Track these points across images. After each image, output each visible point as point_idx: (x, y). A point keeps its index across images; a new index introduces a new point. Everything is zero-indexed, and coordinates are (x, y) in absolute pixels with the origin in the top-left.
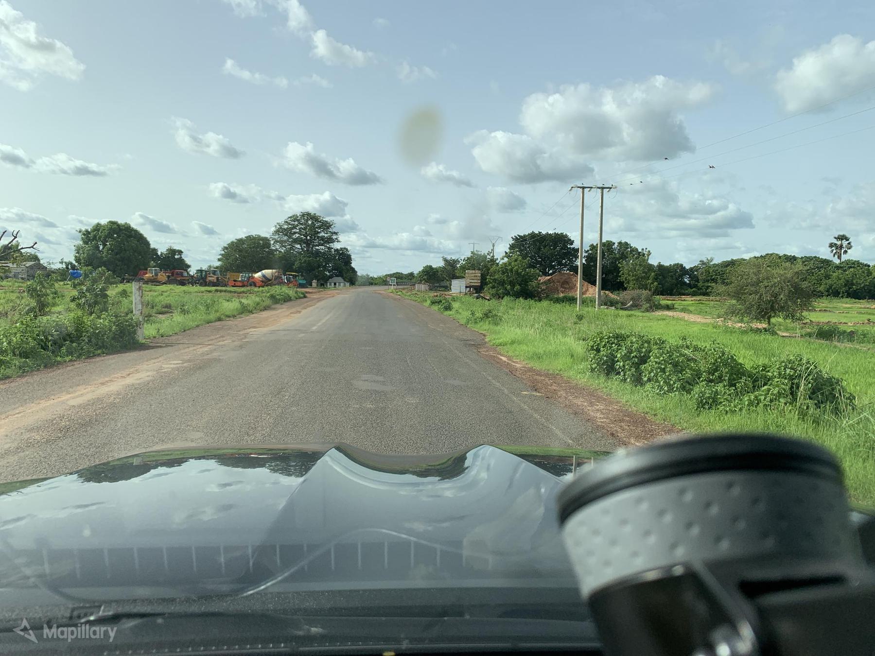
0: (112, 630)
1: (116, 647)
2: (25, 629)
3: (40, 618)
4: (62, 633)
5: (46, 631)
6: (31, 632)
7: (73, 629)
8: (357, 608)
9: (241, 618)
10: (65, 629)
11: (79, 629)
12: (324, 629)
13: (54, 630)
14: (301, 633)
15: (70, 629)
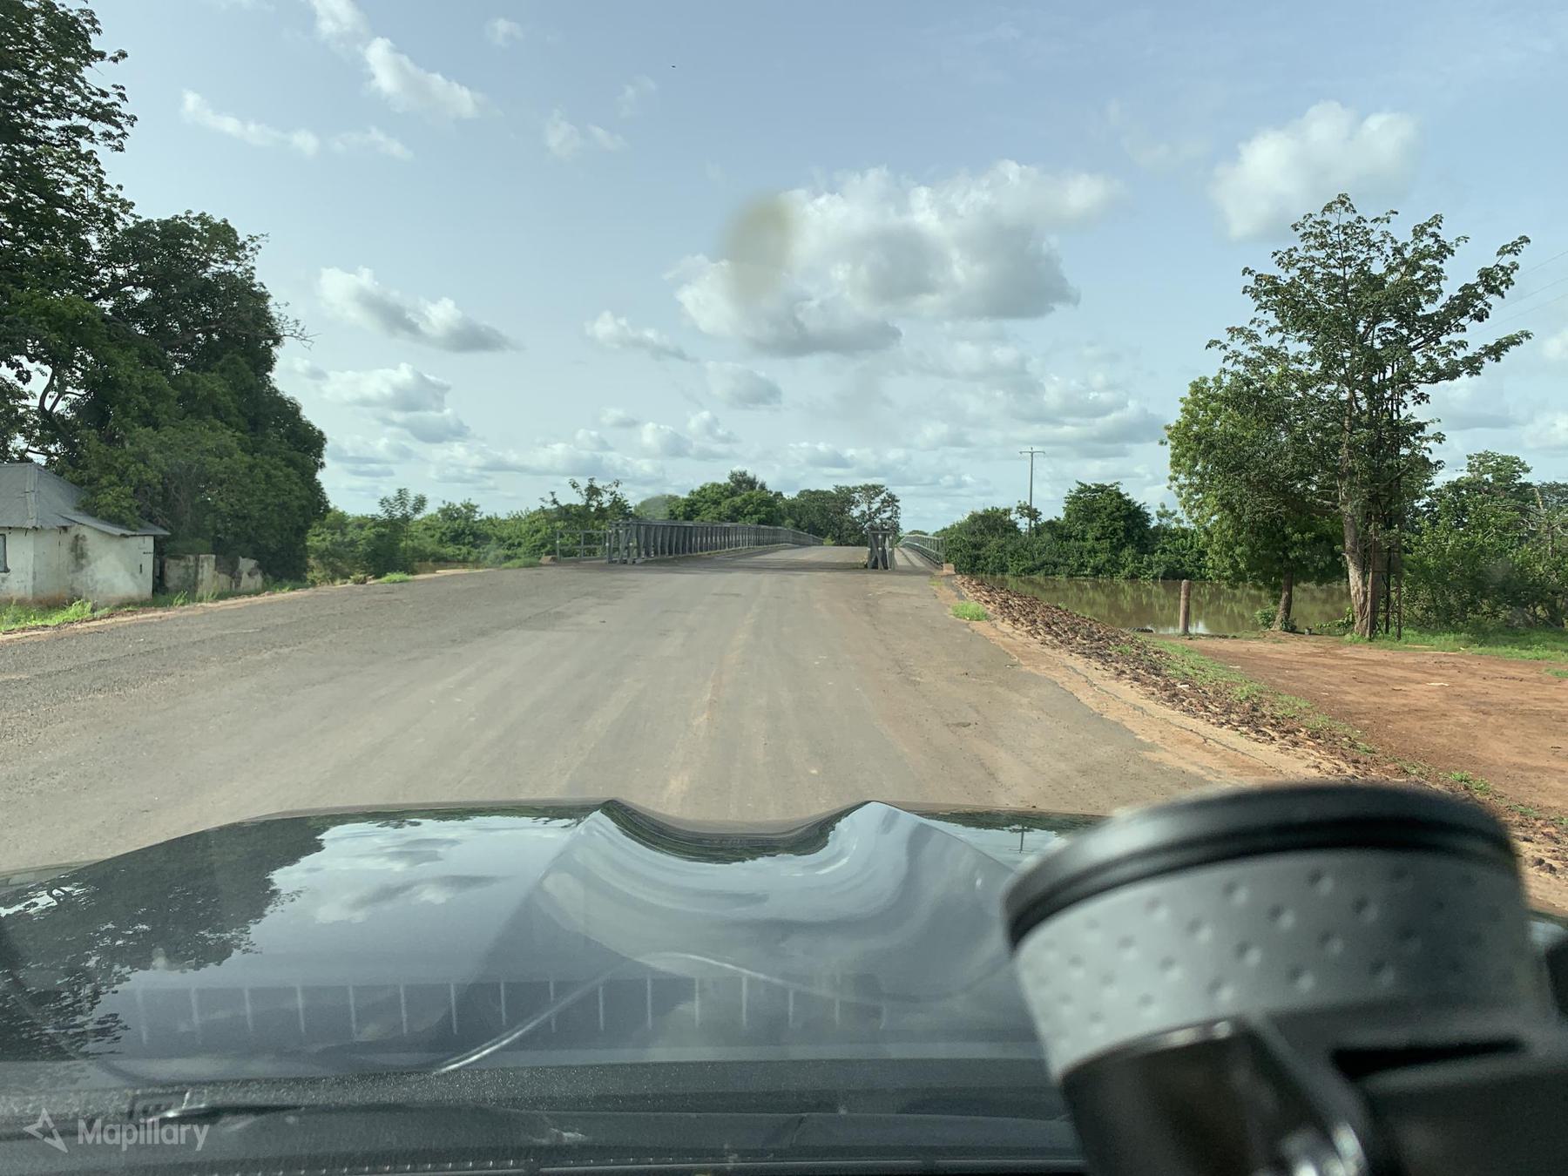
1: (213, 1167)
3: (76, 1114)
8: (645, 1097)
12: (586, 1135)
14: (545, 1142)
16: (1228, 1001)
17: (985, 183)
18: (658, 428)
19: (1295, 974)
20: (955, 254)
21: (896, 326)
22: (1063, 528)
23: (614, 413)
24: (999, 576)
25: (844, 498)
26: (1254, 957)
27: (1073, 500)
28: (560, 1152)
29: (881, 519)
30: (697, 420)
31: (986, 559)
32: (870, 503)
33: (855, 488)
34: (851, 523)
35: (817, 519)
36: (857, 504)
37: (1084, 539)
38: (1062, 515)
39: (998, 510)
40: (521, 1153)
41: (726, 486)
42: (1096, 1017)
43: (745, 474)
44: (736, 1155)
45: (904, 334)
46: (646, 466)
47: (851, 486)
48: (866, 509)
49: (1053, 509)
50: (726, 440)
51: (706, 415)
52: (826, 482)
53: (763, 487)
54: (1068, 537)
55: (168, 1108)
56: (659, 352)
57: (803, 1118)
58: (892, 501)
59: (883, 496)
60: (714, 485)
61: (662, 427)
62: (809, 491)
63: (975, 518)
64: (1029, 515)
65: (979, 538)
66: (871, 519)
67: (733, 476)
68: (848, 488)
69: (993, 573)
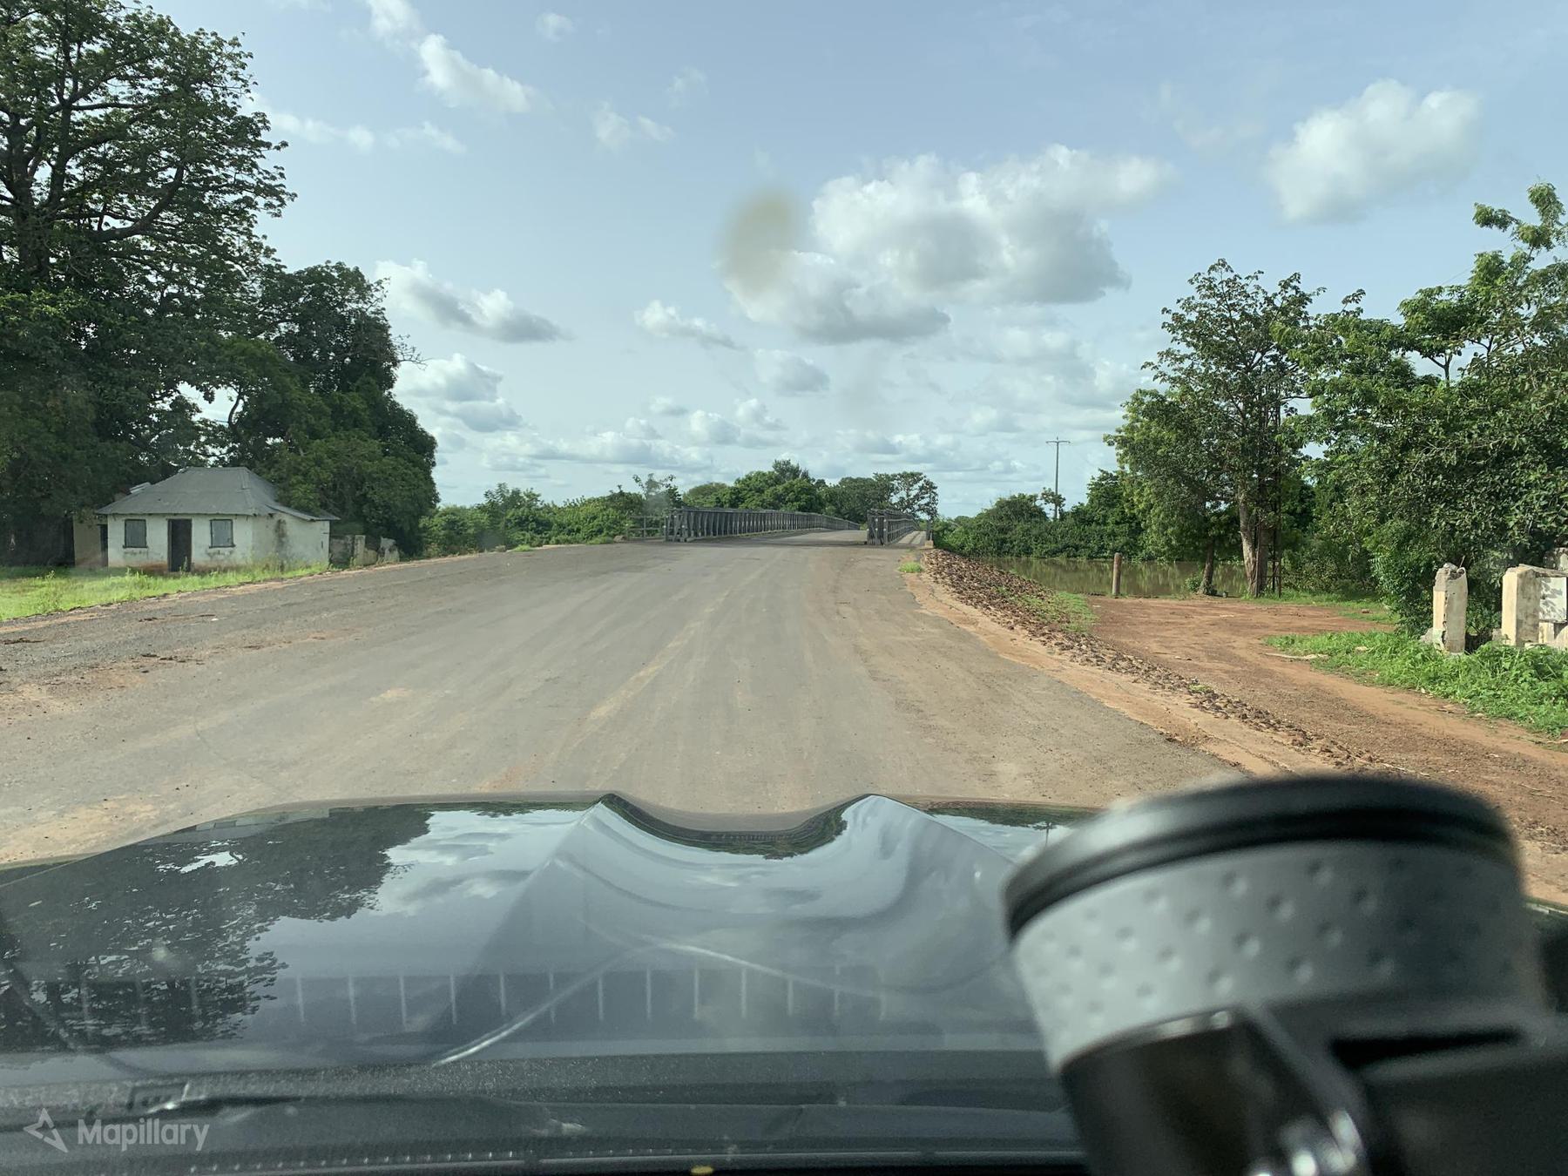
0: (201, 1129)
2: (44, 1128)
4: (112, 1134)
5: (82, 1129)
6: (55, 1132)
7: (131, 1126)
8: (645, 1088)
9: (436, 1105)
10: (116, 1127)
11: (142, 1127)
13: (97, 1128)
14: (545, 1132)
15: (125, 1127)
16: (1227, 990)
17: (1035, 167)
18: (707, 416)
19: (1293, 964)
20: (1004, 240)
21: (945, 311)
22: (1085, 513)
23: (662, 402)
24: (1024, 558)
25: (883, 486)
26: (1253, 948)
27: (1096, 487)
28: (562, 1143)
30: (743, 409)
31: (1011, 542)
32: (908, 489)
33: (895, 476)
37: (1105, 524)
38: (1086, 501)
39: (1024, 497)
40: (519, 1144)
41: (770, 475)
42: (1095, 1007)
44: (735, 1146)
45: (952, 320)
46: (694, 454)
47: (890, 474)
48: (905, 496)
49: (1076, 495)
50: (774, 427)
51: (753, 402)
52: (866, 471)
54: (1089, 522)
55: (168, 1099)
56: (707, 341)
57: (801, 1110)
58: (929, 487)
59: (921, 483)
60: (759, 473)
61: (710, 415)
62: (851, 479)
63: (1002, 505)
64: (1054, 501)
65: (1005, 523)
66: (909, 506)
67: (777, 465)
68: (887, 476)
69: (1018, 556)
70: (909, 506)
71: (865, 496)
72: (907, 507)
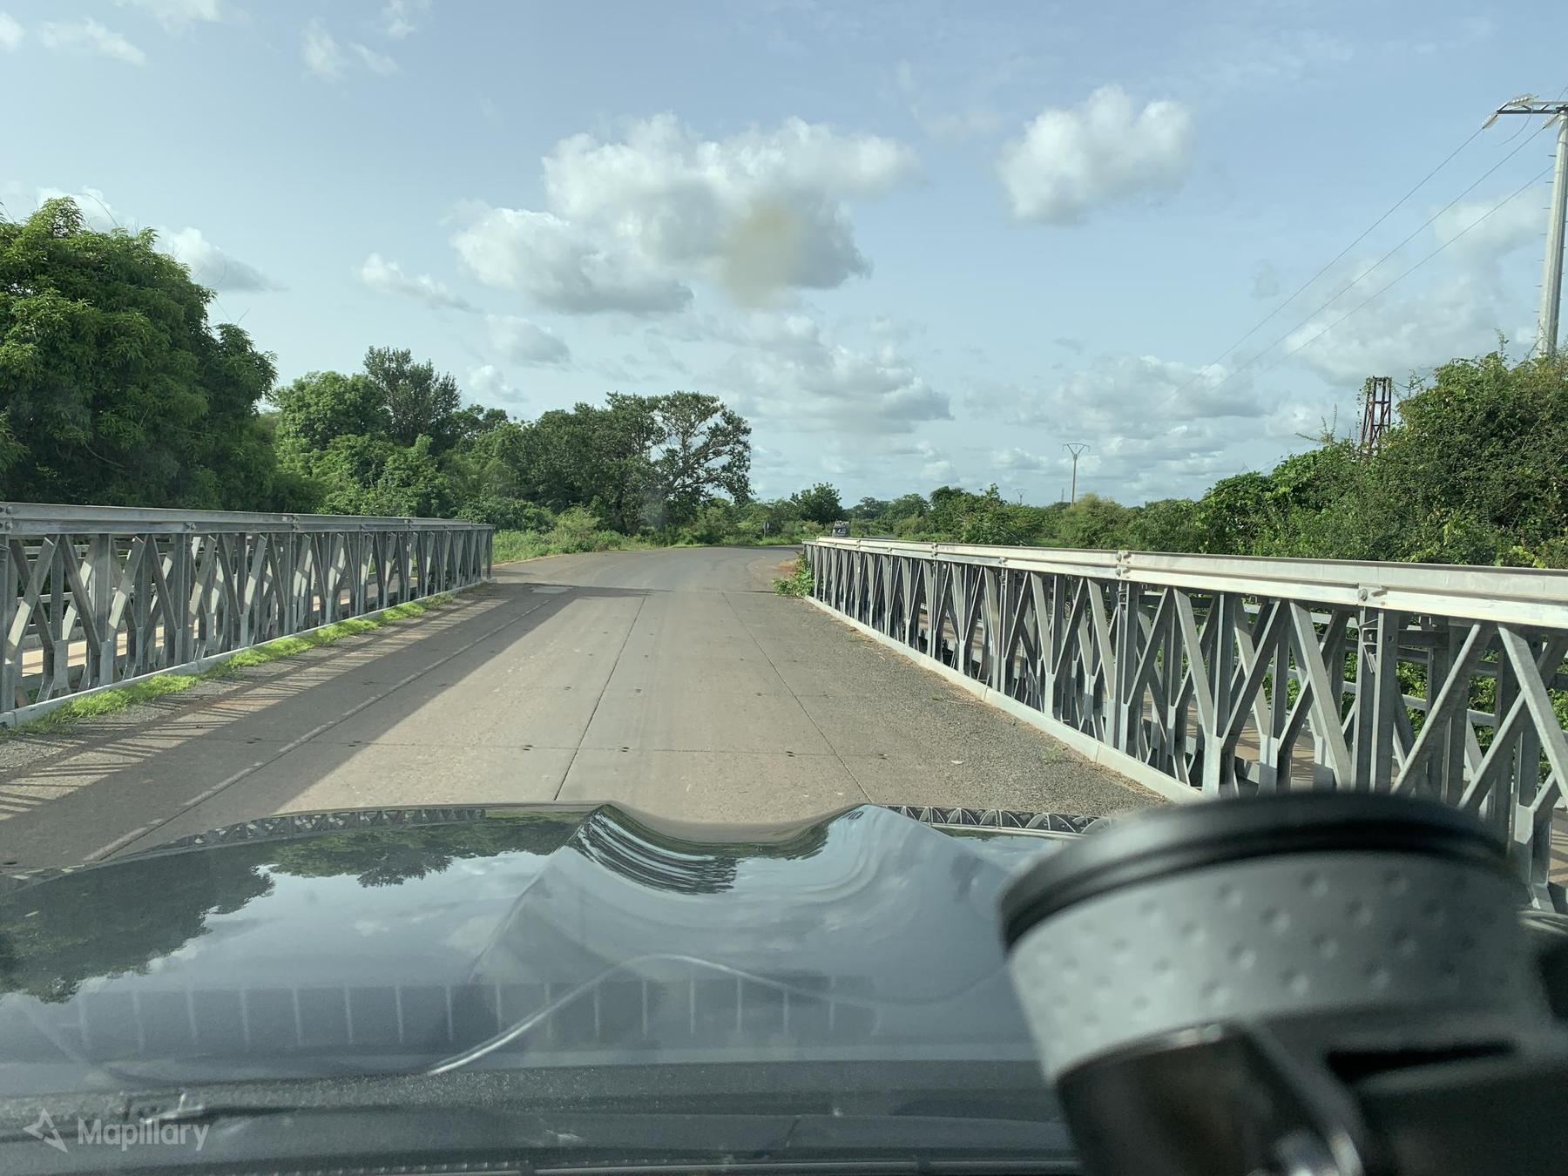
29: (708, 471)
32: (687, 434)
34: (644, 474)
35: (566, 463)
36: (660, 436)
43: (406, 357)
48: (677, 447)
53: (448, 392)
58: (734, 429)
59: (716, 420)
66: (688, 470)
68: (640, 403)
70: (688, 470)
71: (585, 442)
72: (682, 472)
